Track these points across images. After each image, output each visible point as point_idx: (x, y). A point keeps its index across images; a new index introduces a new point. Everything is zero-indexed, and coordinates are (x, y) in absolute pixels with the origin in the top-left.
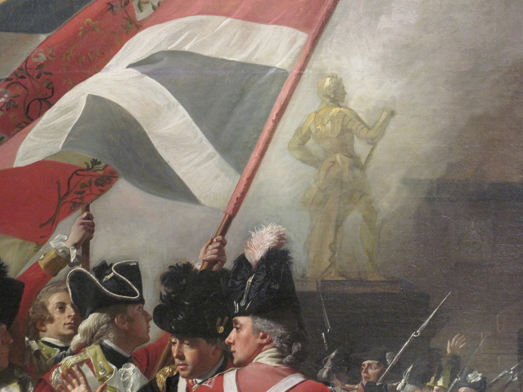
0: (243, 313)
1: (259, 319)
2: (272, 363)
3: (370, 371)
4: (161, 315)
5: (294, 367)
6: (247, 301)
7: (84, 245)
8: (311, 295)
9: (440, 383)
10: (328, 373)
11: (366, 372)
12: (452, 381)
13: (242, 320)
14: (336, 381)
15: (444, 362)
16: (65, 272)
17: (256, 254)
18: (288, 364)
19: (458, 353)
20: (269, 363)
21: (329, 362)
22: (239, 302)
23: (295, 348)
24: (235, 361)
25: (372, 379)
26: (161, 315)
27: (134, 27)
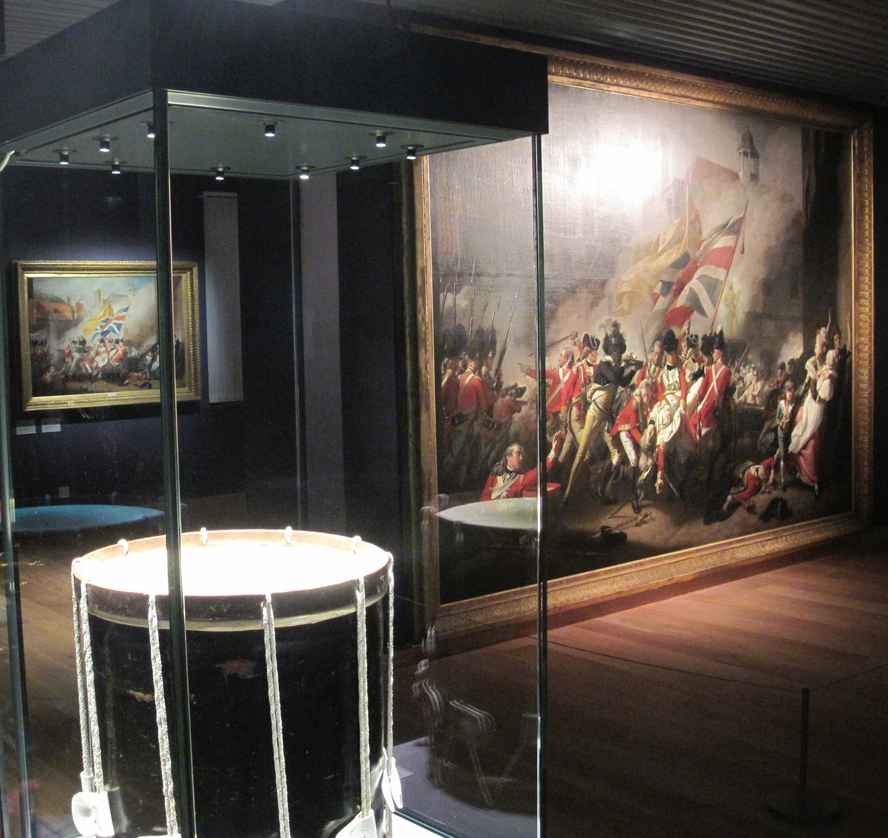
4: (702, 349)
7: (689, 329)
16: (685, 337)
17: (718, 332)
26: (702, 349)
27: (697, 268)
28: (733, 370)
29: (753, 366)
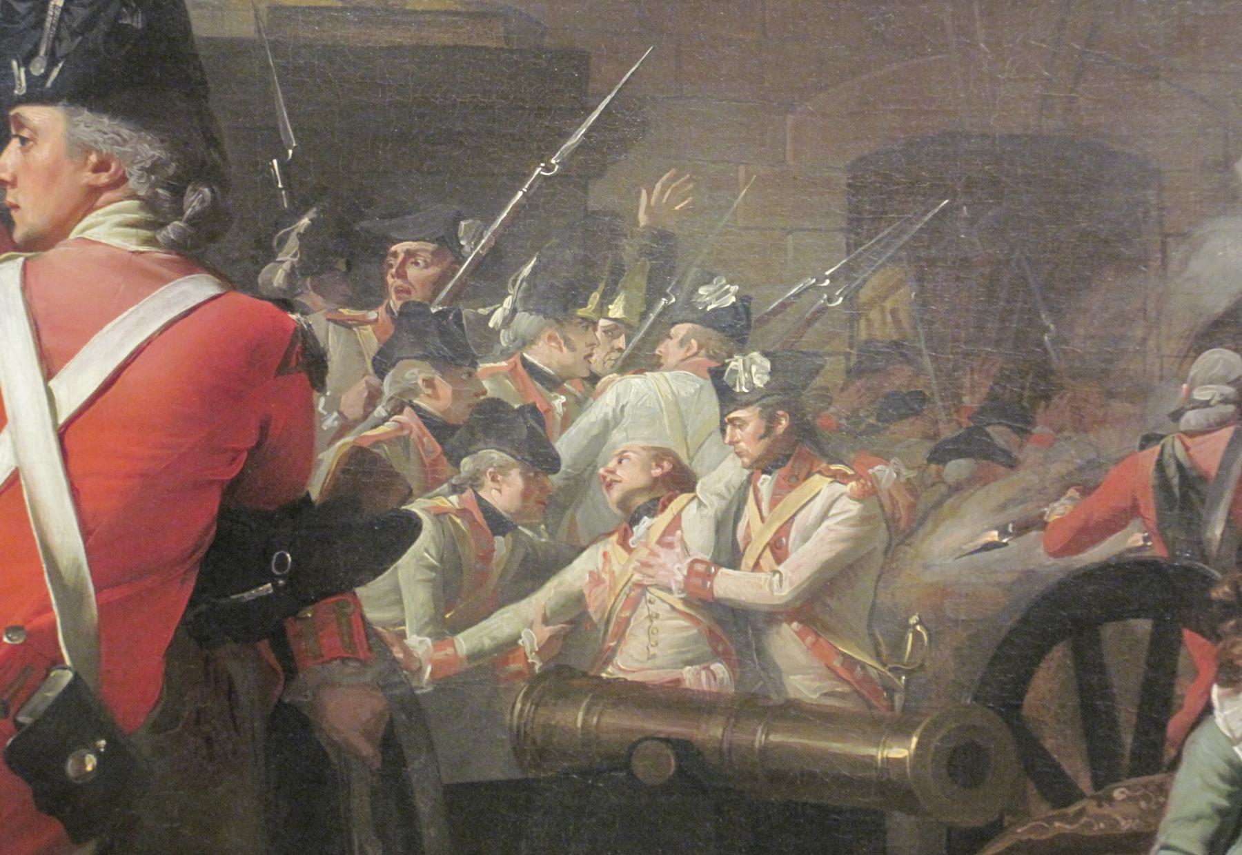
0: (37, 95)
1: (86, 115)
2: (128, 242)
3: (412, 272)
5: (191, 254)
6: (52, 61)
8: (235, 48)
9: (616, 310)
10: (291, 275)
11: (401, 274)
12: (650, 306)
13: (35, 115)
14: (310, 298)
15: (629, 250)
18: (172, 246)
19: (671, 225)
20: (116, 242)
21: (293, 244)
22: (26, 61)
23: (196, 199)
24: (18, 234)
25: (416, 297)
28: (346, 337)
29: (718, 296)
